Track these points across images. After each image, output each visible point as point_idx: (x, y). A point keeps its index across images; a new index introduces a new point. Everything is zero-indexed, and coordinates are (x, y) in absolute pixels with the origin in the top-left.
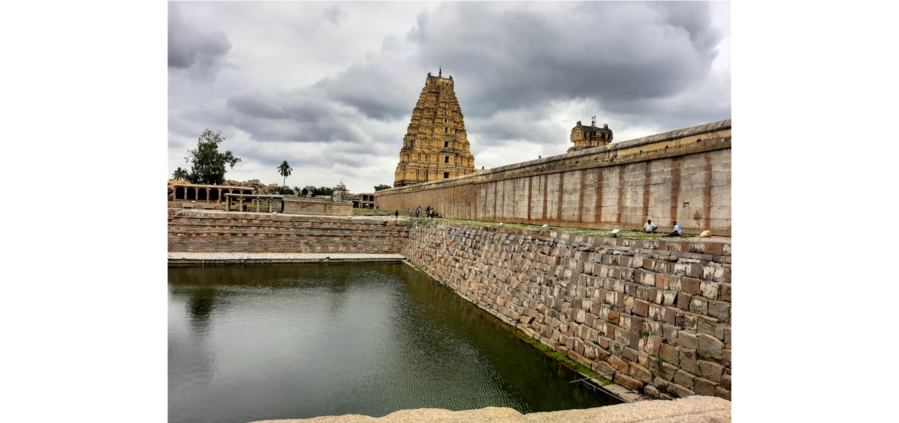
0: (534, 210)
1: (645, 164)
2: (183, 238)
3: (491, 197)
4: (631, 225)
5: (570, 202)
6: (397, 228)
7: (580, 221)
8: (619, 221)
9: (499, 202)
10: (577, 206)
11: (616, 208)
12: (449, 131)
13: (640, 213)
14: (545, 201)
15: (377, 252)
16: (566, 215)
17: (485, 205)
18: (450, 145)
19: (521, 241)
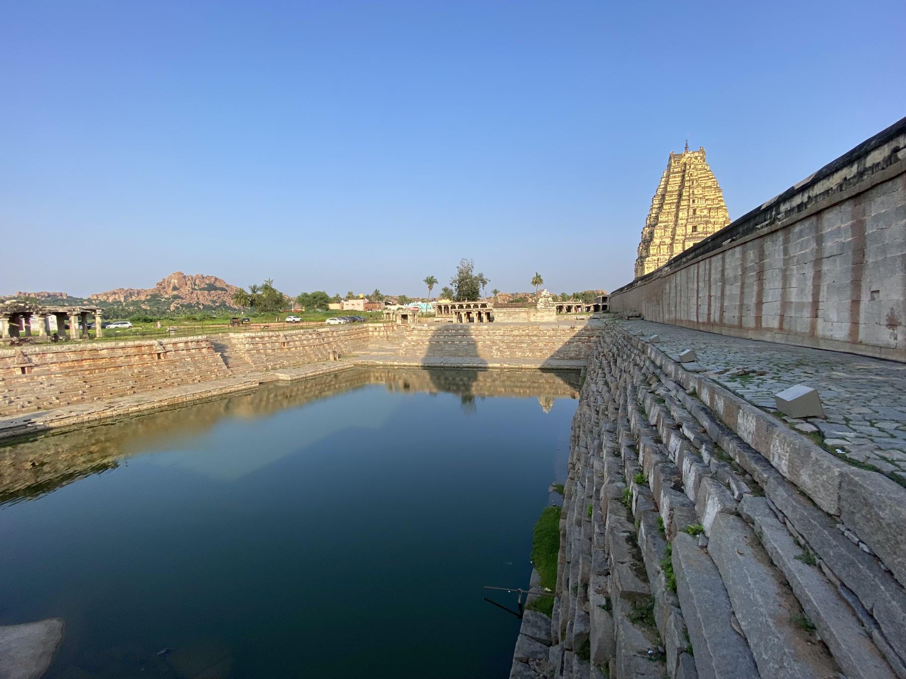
1: (814, 219)
2: (414, 346)
4: (796, 334)
6: (587, 333)
7: (740, 326)
8: (781, 328)
9: (678, 299)
11: (778, 304)
12: (698, 213)
13: (807, 313)
14: (710, 296)
15: (563, 359)
18: (700, 229)
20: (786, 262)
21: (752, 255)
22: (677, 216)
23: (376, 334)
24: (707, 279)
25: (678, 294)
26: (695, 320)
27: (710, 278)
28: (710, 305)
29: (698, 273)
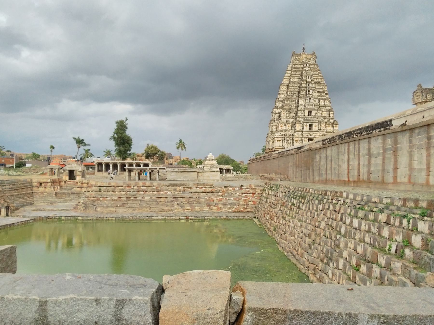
0: (351, 173)
1: (426, 127)
3: (323, 162)
4: (418, 185)
5: (376, 165)
7: (383, 182)
8: (410, 182)
9: (329, 166)
10: (381, 168)
11: (407, 169)
13: (424, 174)
14: (359, 164)
16: (373, 177)
17: (320, 169)
18: (313, 113)
19: (325, 200)
20: (411, 147)
21: (389, 141)
22: (298, 102)
23: (41, 189)
24: (356, 153)
25: (329, 162)
26: (347, 179)
27: (359, 153)
28: (359, 170)
29: (348, 149)
